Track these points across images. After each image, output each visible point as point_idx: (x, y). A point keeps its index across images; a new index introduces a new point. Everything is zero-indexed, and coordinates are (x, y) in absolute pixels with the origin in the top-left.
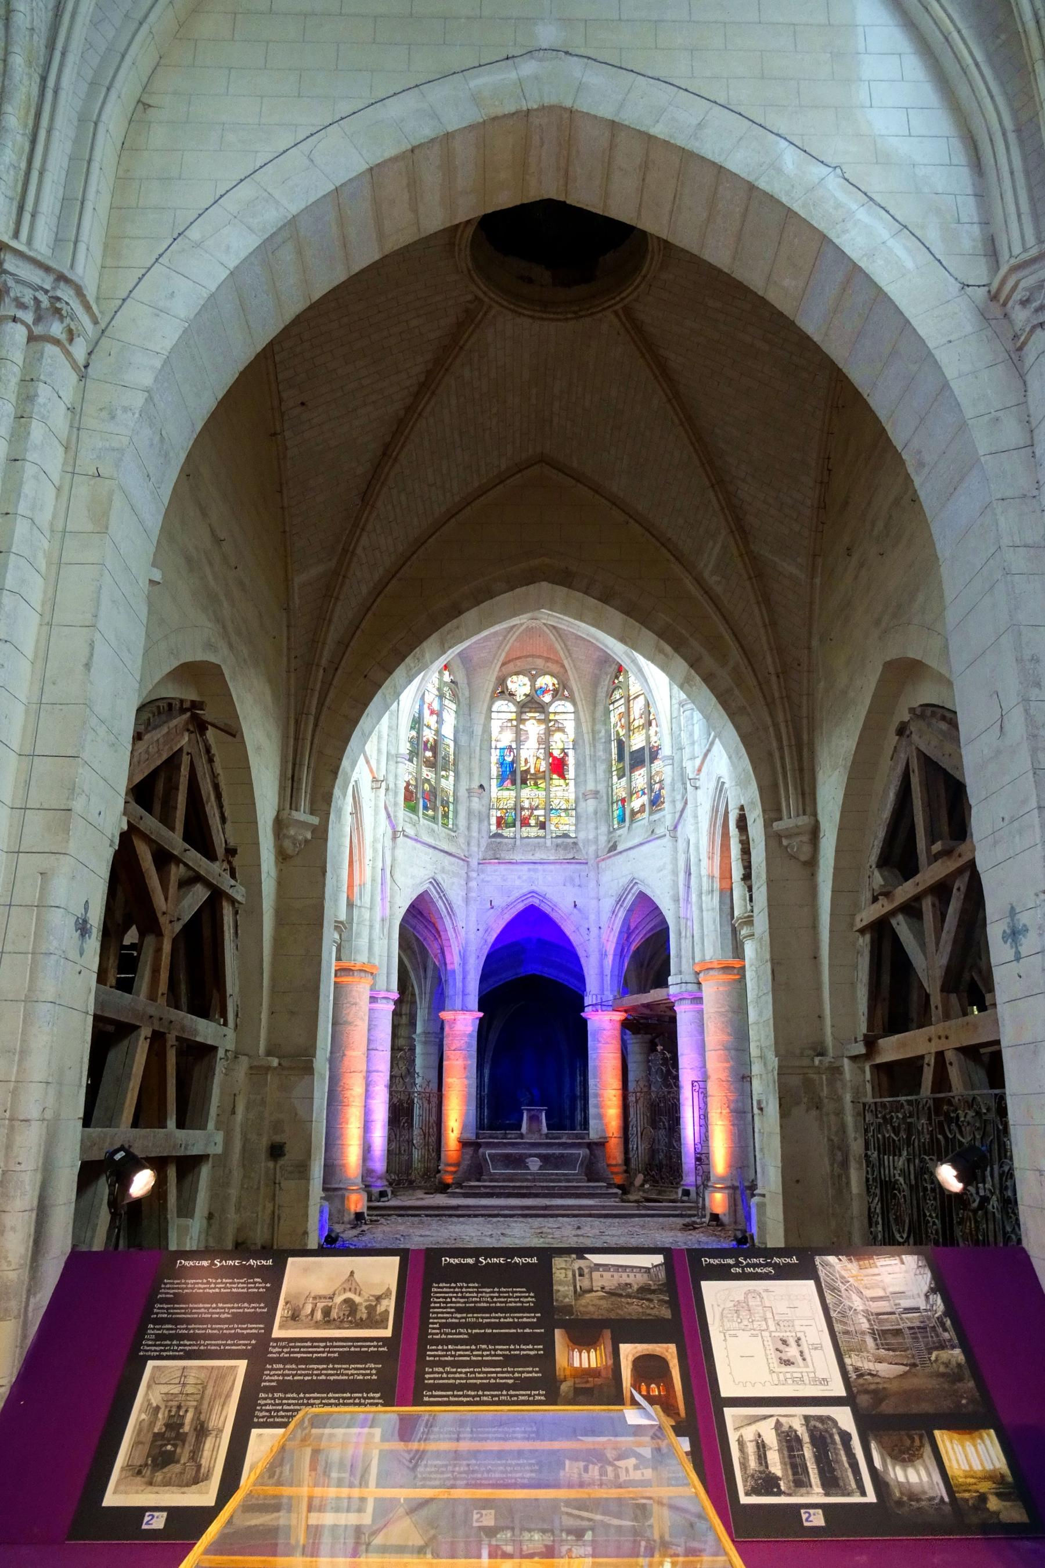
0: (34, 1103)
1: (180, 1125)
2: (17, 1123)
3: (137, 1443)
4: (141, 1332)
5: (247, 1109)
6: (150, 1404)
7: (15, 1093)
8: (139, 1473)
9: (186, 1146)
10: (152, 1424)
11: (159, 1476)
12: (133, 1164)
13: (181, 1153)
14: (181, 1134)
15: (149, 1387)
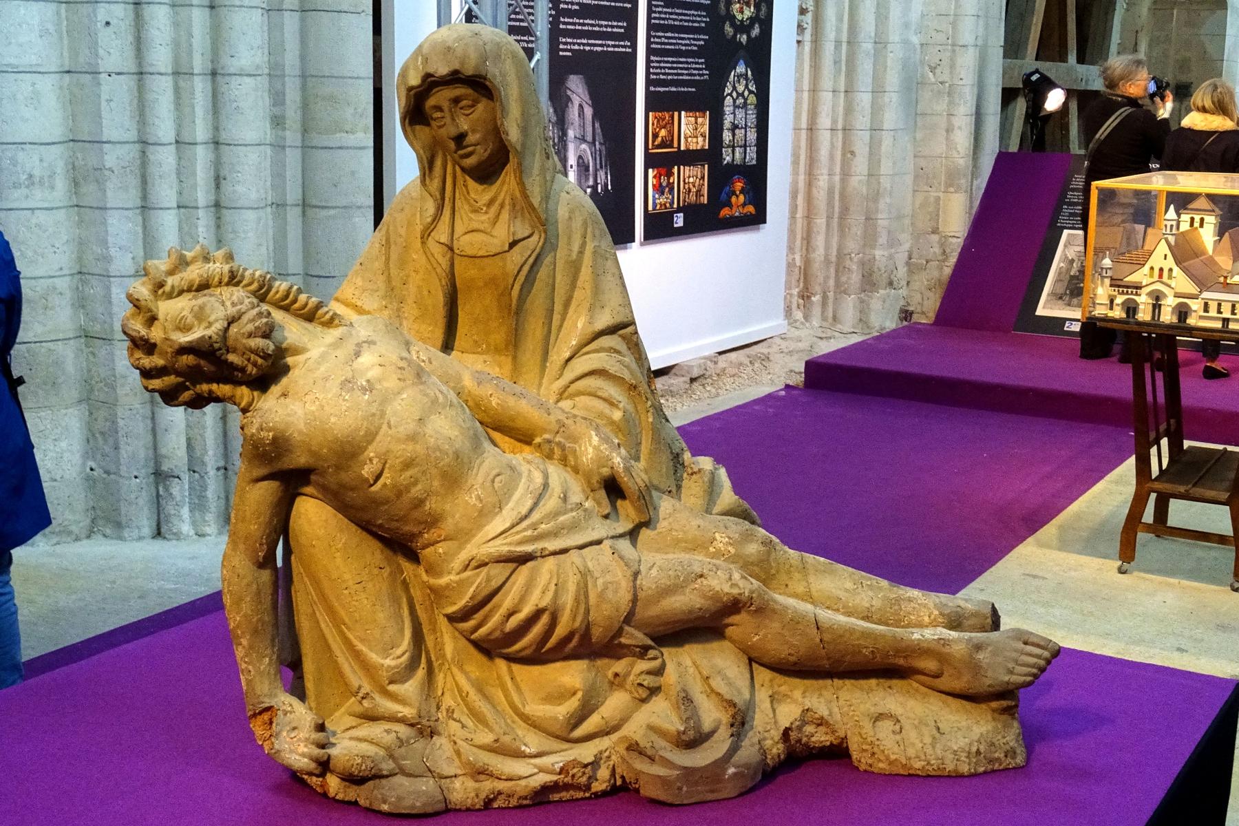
0: (968, 32)
1: (1081, 60)
2: (957, 48)
3: (1058, 280)
4: (1058, 211)
5: (1150, 46)
6: (1066, 257)
7: (954, 25)
8: (1061, 298)
9: (1087, 81)
10: (1069, 270)
11: (1075, 301)
12: (1047, 84)
13: (1082, 87)
14: (1082, 69)
15: (1065, 246)
